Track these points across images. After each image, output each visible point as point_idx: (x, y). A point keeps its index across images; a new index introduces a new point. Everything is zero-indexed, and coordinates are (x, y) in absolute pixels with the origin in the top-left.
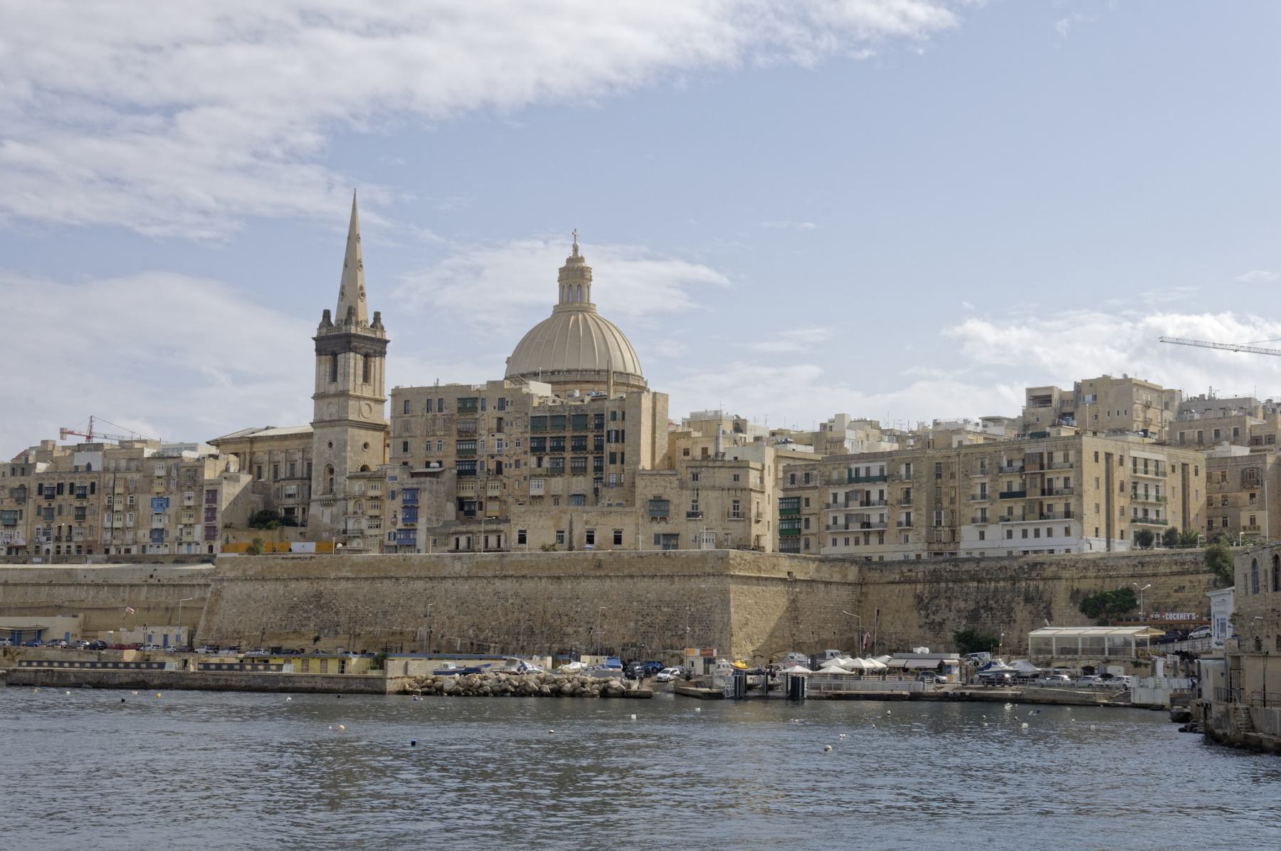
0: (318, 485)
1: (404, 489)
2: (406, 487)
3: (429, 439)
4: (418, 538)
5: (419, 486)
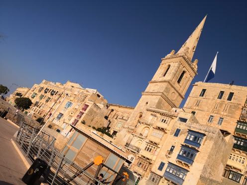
0: (131, 121)
1: (190, 130)
2: (192, 129)
3: (213, 115)
4: (186, 178)
5: (206, 133)
